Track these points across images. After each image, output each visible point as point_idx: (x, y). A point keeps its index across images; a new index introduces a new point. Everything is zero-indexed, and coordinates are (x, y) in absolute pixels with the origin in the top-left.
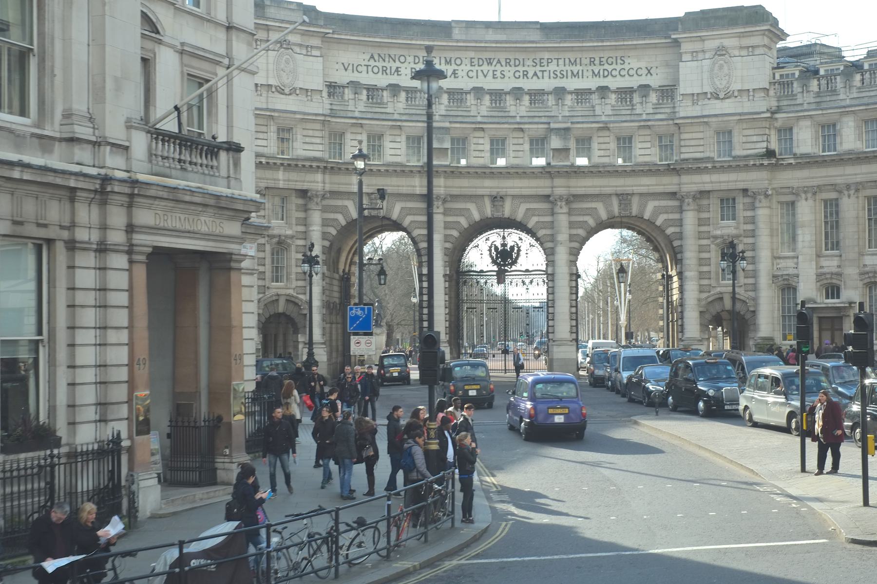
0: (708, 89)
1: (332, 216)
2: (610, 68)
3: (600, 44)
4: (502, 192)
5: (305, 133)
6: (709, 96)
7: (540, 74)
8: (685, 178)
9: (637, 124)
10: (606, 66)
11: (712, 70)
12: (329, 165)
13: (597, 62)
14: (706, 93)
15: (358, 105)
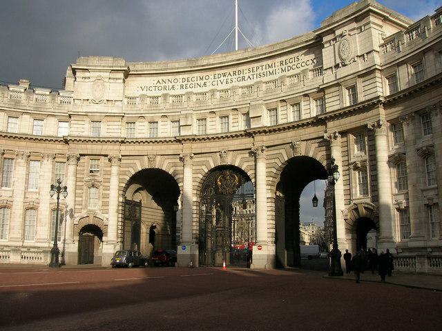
0: (338, 61)
1: (127, 169)
2: (291, 65)
3: (283, 51)
4: (226, 148)
5: (109, 123)
6: (340, 65)
7: (251, 77)
8: (330, 124)
9: (302, 94)
10: (289, 64)
11: (339, 48)
12: (120, 140)
13: (284, 63)
14: (338, 64)
15: (141, 107)
